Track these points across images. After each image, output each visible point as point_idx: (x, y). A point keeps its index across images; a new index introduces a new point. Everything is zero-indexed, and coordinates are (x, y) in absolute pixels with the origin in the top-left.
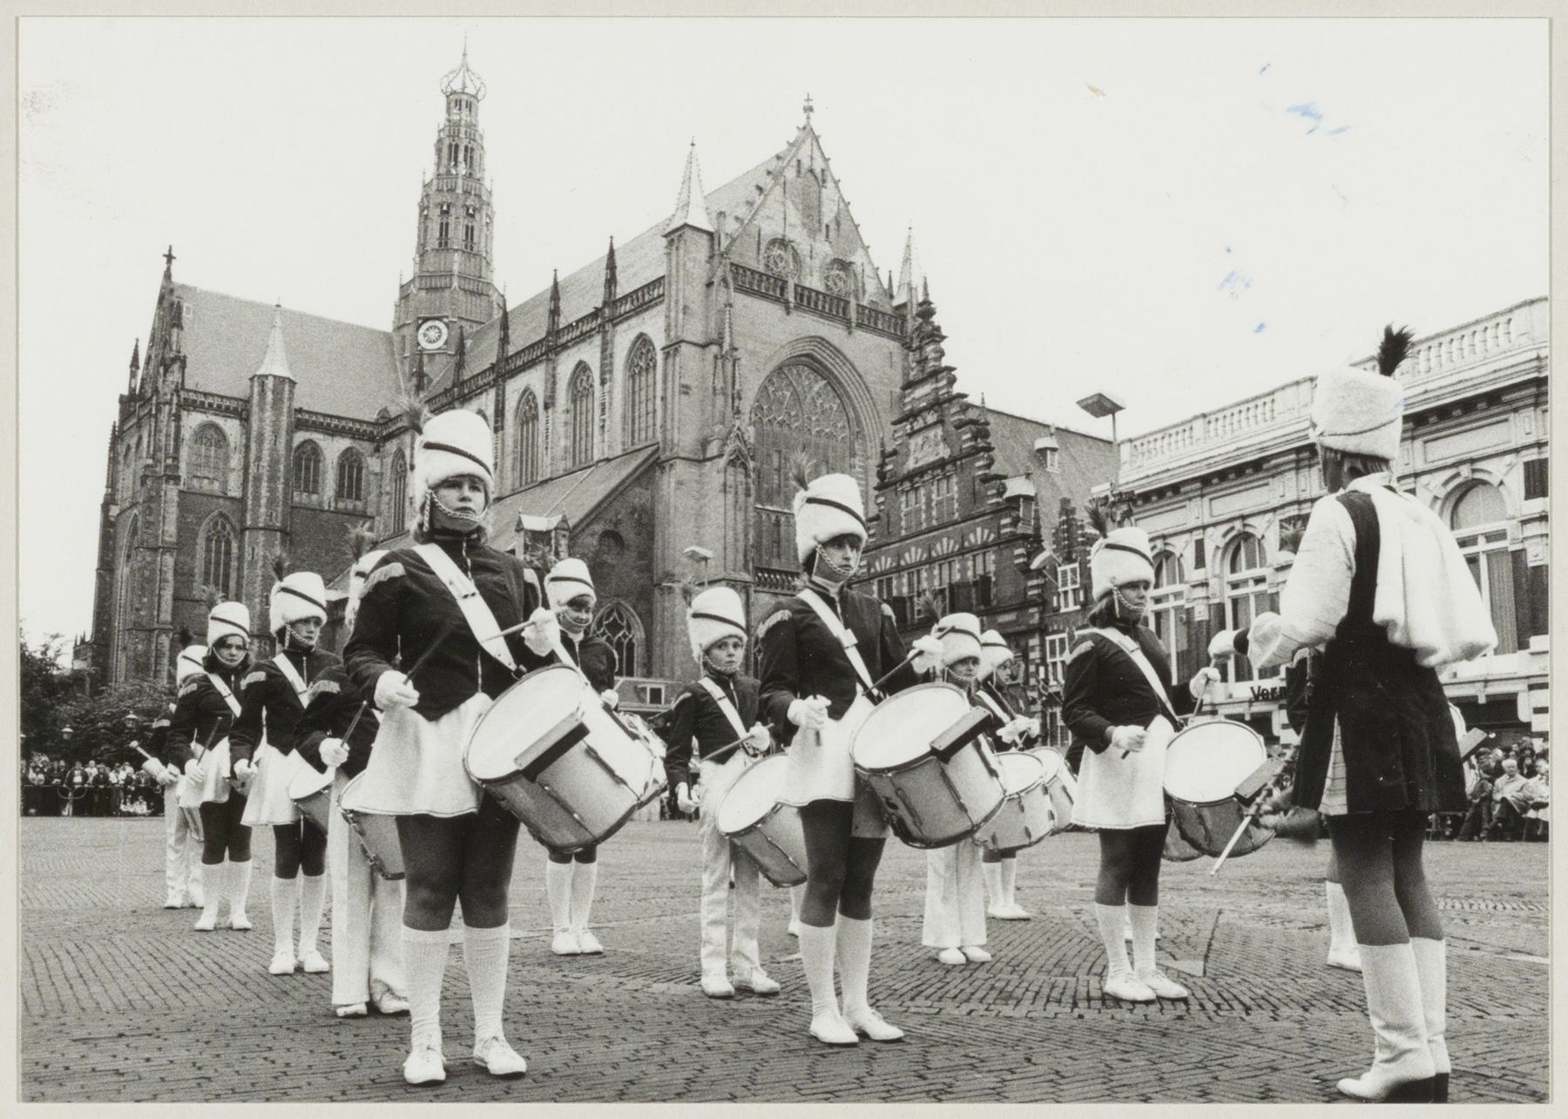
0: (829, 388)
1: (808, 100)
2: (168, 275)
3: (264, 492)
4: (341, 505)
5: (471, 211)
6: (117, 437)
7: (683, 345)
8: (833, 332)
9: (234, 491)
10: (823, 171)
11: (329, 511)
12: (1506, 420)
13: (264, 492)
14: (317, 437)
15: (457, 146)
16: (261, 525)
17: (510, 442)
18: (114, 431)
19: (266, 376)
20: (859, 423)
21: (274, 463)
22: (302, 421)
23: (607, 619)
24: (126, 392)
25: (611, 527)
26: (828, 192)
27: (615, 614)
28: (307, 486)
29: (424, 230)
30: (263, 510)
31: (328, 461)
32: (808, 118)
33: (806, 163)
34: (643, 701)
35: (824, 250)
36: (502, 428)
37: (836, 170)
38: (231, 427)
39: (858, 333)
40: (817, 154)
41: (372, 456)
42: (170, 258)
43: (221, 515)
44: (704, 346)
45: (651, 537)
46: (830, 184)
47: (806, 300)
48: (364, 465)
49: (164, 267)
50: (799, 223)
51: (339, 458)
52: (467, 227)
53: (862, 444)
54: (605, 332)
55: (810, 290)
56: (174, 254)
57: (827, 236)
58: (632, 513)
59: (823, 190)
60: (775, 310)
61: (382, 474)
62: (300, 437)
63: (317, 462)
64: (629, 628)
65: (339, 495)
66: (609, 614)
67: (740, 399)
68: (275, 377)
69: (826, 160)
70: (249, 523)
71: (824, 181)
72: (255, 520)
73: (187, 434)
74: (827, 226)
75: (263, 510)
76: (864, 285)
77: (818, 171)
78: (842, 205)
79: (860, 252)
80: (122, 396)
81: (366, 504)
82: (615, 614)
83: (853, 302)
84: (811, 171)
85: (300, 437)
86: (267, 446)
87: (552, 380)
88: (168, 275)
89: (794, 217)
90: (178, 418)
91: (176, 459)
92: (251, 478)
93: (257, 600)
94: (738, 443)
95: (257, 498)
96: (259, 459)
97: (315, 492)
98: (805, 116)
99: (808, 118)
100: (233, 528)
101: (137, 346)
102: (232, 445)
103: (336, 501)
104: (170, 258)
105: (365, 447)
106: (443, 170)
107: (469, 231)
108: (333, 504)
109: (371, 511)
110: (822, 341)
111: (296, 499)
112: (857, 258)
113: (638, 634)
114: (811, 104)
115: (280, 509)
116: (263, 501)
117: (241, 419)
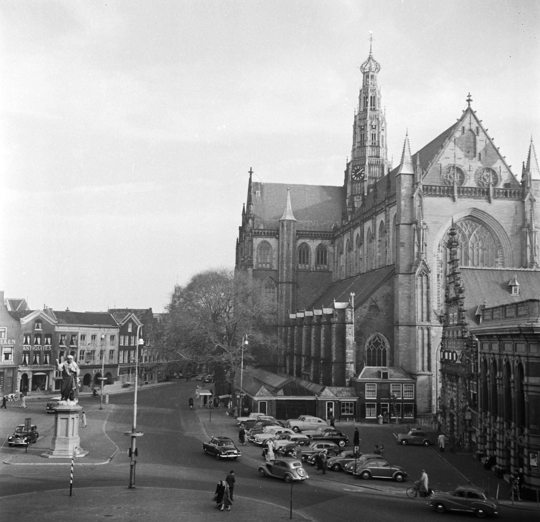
0: (484, 228)
1: (469, 96)
2: (250, 179)
3: (285, 268)
4: (318, 268)
5: (374, 127)
6: (238, 245)
7: (401, 226)
8: (481, 204)
9: (275, 268)
10: (477, 128)
11: (313, 271)
12: (523, 343)
13: (285, 268)
14: (307, 241)
15: (367, 98)
16: (284, 281)
17: (365, 250)
18: (237, 241)
19: (284, 220)
20: (499, 243)
21: (288, 255)
22: (300, 234)
23: (373, 341)
24: (241, 226)
25: (374, 304)
26: (481, 137)
27: (377, 338)
28: (304, 262)
29: (354, 138)
30: (284, 275)
31: (312, 250)
32: (469, 105)
33: (467, 127)
34: (379, 377)
35: (476, 165)
36: (363, 243)
37: (485, 125)
38: (272, 241)
39: (495, 202)
40: (473, 121)
41: (330, 245)
42: (251, 172)
43: (270, 277)
44: (411, 224)
45: (392, 305)
46: (481, 133)
47: (465, 192)
48: (328, 250)
49: (249, 177)
50: (463, 156)
51: (316, 248)
52: (373, 134)
53: (502, 252)
54: (386, 210)
55: (467, 188)
56: (252, 171)
57: (480, 159)
58: (383, 297)
59: (477, 137)
60: (447, 200)
61: (334, 253)
62: (300, 242)
63: (308, 251)
64: (384, 343)
65: (318, 262)
66: (374, 339)
67: (426, 246)
68: (287, 220)
69: (478, 122)
70: (280, 280)
71: (478, 133)
72: (282, 279)
73: (255, 246)
74: (480, 154)
75: (284, 275)
76: (501, 176)
77: (474, 128)
78: (488, 141)
79: (499, 161)
80: (240, 227)
81: (328, 266)
82: (377, 338)
83: (491, 188)
84: (471, 130)
85: (300, 242)
86: (285, 248)
87: (374, 225)
88: (250, 179)
89: (460, 153)
90: (251, 241)
91: (251, 258)
92: (280, 262)
93: (284, 312)
94: (423, 266)
95: (282, 269)
96: (282, 254)
97: (307, 263)
98: (468, 103)
99: (469, 105)
100: (275, 282)
101: (244, 207)
102: (274, 249)
103: (316, 266)
104: (251, 172)
105: (327, 242)
106: (362, 110)
107: (373, 136)
108: (315, 268)
109: (331, 270)
110: (475, 209)
111: (300, 267)
112: (497, 165)
113: (388, 346)
114: (471, 98)
115: (291, 274)
116: (284, 272)
117: (276, 238)
